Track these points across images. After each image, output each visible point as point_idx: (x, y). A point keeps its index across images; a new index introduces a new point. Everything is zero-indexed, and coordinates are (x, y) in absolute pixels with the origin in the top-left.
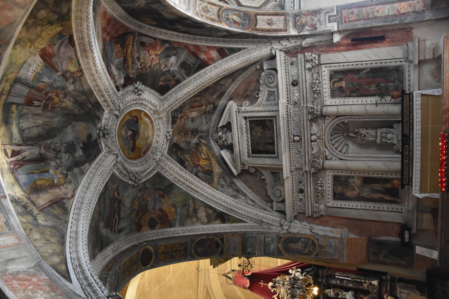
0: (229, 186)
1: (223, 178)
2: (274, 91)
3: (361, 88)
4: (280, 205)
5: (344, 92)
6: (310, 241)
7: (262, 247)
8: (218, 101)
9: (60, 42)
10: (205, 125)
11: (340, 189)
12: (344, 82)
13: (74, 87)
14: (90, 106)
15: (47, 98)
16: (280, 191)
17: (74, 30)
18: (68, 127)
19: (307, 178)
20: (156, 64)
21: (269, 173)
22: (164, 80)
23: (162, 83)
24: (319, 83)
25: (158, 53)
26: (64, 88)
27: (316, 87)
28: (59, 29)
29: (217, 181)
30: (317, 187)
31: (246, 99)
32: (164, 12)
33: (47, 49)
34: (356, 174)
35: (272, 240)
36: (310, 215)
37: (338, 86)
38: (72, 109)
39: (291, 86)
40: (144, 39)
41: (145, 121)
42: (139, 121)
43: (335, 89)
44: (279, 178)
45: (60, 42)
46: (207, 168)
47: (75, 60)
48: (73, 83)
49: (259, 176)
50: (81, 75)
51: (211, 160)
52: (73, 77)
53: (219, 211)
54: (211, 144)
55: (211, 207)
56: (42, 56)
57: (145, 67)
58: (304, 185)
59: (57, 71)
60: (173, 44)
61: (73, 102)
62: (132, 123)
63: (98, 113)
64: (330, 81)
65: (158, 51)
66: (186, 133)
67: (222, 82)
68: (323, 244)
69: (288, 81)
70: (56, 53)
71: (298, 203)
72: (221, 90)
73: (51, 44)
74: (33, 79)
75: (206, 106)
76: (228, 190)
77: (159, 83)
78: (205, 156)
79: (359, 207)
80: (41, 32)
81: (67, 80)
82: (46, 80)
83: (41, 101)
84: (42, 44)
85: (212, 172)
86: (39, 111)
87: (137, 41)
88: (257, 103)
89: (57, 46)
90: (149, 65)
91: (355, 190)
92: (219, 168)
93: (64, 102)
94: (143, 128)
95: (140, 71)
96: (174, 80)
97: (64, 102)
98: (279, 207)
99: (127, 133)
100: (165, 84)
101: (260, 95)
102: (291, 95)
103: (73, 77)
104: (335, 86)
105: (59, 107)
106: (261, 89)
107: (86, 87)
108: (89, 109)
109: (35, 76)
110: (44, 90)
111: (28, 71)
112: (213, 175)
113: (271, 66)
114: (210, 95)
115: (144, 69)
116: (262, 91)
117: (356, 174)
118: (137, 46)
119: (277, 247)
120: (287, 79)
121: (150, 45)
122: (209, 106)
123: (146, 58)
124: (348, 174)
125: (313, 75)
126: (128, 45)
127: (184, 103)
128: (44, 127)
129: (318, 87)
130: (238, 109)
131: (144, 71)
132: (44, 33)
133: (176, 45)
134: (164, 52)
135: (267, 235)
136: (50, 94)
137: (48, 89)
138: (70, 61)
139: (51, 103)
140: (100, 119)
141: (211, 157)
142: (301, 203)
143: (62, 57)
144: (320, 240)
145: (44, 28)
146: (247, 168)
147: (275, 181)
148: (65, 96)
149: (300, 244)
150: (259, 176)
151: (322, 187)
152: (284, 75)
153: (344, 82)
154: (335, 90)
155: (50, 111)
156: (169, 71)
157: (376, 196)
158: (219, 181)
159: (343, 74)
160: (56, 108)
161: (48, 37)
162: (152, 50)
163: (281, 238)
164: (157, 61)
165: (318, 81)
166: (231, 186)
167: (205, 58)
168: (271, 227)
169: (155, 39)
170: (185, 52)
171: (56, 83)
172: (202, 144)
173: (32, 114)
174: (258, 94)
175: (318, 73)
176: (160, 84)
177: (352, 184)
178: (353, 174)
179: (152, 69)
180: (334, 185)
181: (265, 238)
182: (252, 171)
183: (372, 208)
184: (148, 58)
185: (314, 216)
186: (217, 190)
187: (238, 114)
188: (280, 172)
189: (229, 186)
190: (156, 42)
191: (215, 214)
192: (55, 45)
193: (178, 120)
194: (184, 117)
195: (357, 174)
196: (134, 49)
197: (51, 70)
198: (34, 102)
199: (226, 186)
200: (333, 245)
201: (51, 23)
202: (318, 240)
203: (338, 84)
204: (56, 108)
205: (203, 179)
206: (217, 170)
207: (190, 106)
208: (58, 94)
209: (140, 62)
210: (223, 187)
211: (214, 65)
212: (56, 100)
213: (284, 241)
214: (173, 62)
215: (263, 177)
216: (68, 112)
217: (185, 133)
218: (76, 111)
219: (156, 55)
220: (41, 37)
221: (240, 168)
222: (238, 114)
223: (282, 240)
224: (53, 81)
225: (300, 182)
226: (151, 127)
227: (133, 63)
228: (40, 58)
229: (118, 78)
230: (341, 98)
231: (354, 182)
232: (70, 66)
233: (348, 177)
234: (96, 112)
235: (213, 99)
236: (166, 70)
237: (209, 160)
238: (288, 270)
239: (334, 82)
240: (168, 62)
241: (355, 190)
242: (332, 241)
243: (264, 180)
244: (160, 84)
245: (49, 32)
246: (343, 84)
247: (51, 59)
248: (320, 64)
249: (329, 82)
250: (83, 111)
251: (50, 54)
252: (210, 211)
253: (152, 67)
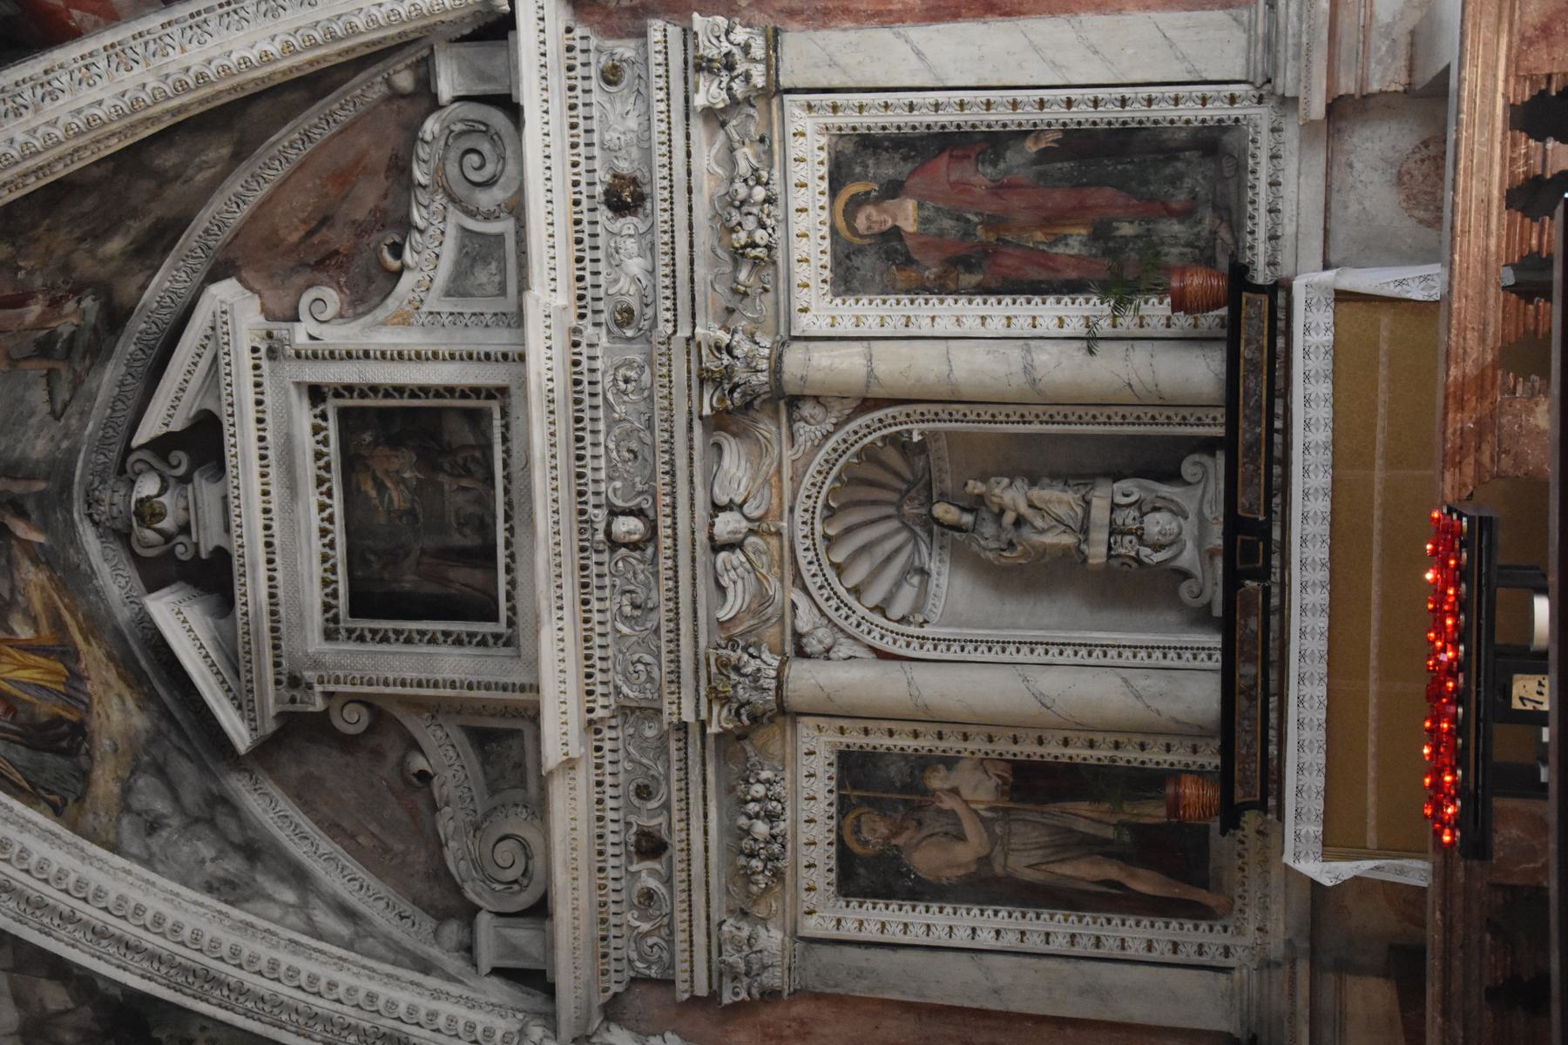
0: (192, 821)
1: (160, 771)
2: (500, 237)
3: (1006, 243)
4: (522, 935)
5: (908, 261)
8: (140, 279)
10: (41, 428)
11: (875, 831)
12: (910, 205)
16: (524, 846)
19: (685, 769)
21: (458, 736)
24: (769, 200)
27: (750, 223)
29: (116, 789)
30: (743, 821)
31: (323, 277)
34: (970, 746)
36: (702, 990)
37: (876, 229)
39: (604, 214)
43: (857, 240)
44: (520, 766)
46: (46, 709)
49: (393, 757)
51: (76, 655)
53: (118, 992)
54: (80, 550)
55: (58, 969)
58: (666, 806)
64: (834, 191)
67: (167, 159)
69: (583, 179)
71: (631, 918)
72: (158, 210)
75: (55, 303)
76: (186, 849)
78: (37, 631)
79: (986, 939)
85: (80, 731)
88: (392, 303)
91: (961, 838)
92: (131, 704)
98: (514, 950)
101: (408, 256)
102: (601, 267)
104: (861, 223)
106: (417, 216)
112: (88, 753)
113: (483, 77)
114: (77, 233)
116: (421, 232)
117: (970, 746)
120: (582, 168)
122: (70, 306)
124: (926, 743)
125: (732, 150)
129: (763, 226)
130: (270, 335)
141: (78, 638)
142: (647, 918)
146: (319, 705)
147: (493, 789)
150: (393, 757)
151: (771, 817)
152: (560, 141)
153: (910, 205)
154: (860, 251)
157: (1084, 871)
158: (127, 790)
159: (905, 159)
165: (759, 193)
166: (212, 823)
172: (17, 551)
174: (397, 250)
175: (762, 140)
177: (948, 803)
178: (952, 744)
180: (844, 806)
182: (353, 721)
183: (1059, 944)
185: (727, 998)
186: (115, 848)
187: (265, 365)
188: (528, 730)
189: (197, 820)
191: (87, 1012)
195: (977, 745)
199: (175, 822)
203: (875, 216)
205: (17, 777)
206: (116, 716)
210: (153, 826)
211: (108, 37)
215: (419, 763)
221: (271, 701)
222: (265, 365)
225: (644, 792)
230: (892, 299)
231: (955, 791)
233: (924, 763)
235: (103, 262)
237: (64, 652)
239: (856, 203)
241: (961, 838)
243: (424, 777)
246: (906, 215)
248: (775, 91)
249: (825, 200)
252: (55, 996)
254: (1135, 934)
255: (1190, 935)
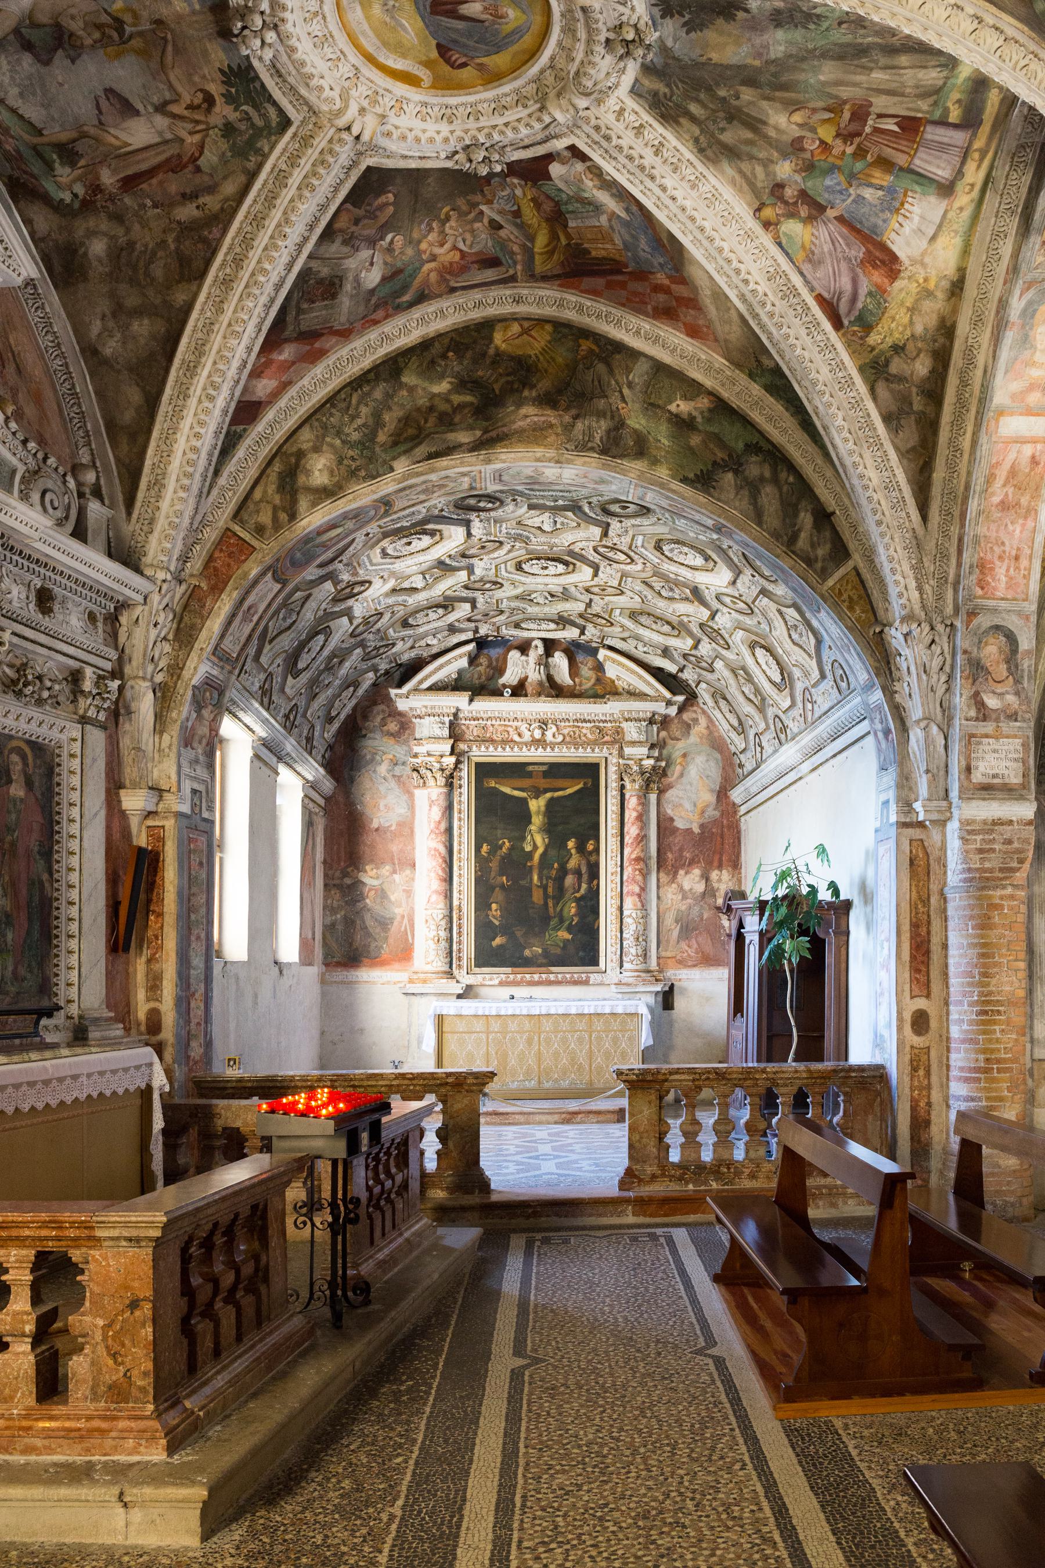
9: (860, 305)
13: (775, 174)
14: (694, 108)
15: (857, 140)
17: (840, 346)
18: (780, 55)
20: (426, 237)
22: (378, 213)
23: (382, 199)
25: (427, 267)
26: (809, 168)
28: (874, 339)
32: (553, 420)
33: (886, 281)
38: (764, 104)
40: (490, 274)
41: (404, 56)
42: (434, 54)
45: (860, 305)
47: (800, 256)
48: (779, 186)
50: (758, 210)
52: (786, 203)
56: (894, 258)
57: (462, 215)
59: (840, 219)
60: (391, 311)
61: (765, 123)
62: (471, 43)
63: (650, 84)
65: (431, 271)
66: (115, 35)
67: (142, 328)
70: (858, 270)
73: (879, 293)
74: (905, 195)
77: (395, 196)
80: (911, 323)
81: (803, 194)
82: (868, 193)
83: (876, 130)
84: (901, 290)
86: (880, 103)
87: (515, 263)
89: (863, 291)
90: (452, 223)
93: (800, 125)
94: (405, 30)
95: (478, 198)
96: (341, 231)
97: (800, 125)
99: (485, 8)
100: (370, 205)
103: (786, 203)
105: (814, 110)
107: (730, 171)
108: (697, 100)
109: (902, 204)
110: (871, 165)
111: (922, 217)
115: (464, 208)
118: (512, 253)
121: (463, 269)
123: (468, 236)
126: (551, 253)
127: (253, 176)
128: (872, 65)
131: (461, 202)
132: (906, 320)
133: (380, 314)
134: (410, 276)
136: (850, 150)
137: (859, 166)
138: (813, 253)
139: (842, 125)
140: (647, 69)
143: (838, 262)
145: (908, 333)
148: (796, 146)
155: (845, 102)
156: (372, 243)
160: (824, 109)
161: (893, 312)
162: (451, 263)
164: (424, 246)
167: (280, 354)
169: (453, 290)
170: (343, 319)
171: (838, 184)
173: (903, 95)
176: (390, 195)
179: (437, 217)
184: (460, 239)
190: (448, 286)
192: (870, 294)
193: (215, 89)
194: (190, 107)
196: (523, 246)
197: (861, 223)
198: (896, 128)
201: (898, 349)
204: (824, 109)
207: (198, 170)
208: (822, 152)
209: (486, 221)
212: (826, 133)
214: (368, 271)
216: (777, 94)
217: (121, 31)
218: (747, 94)
219: (433, 258)
220: (908, 309)
224: (847, 190)
226: (363, 41)
227: (517, 214)
228: (899, 253)
229: (581, 181)
232: (807, 238)
234: (663, 89)
235: (91, 234)
236: (382, 238)
240: (386, 263)
244: (390, 195)
245: (893, 325)
247: (868, 252)
250: (722, 93)
251: (875, 266)
253: (434, 225)
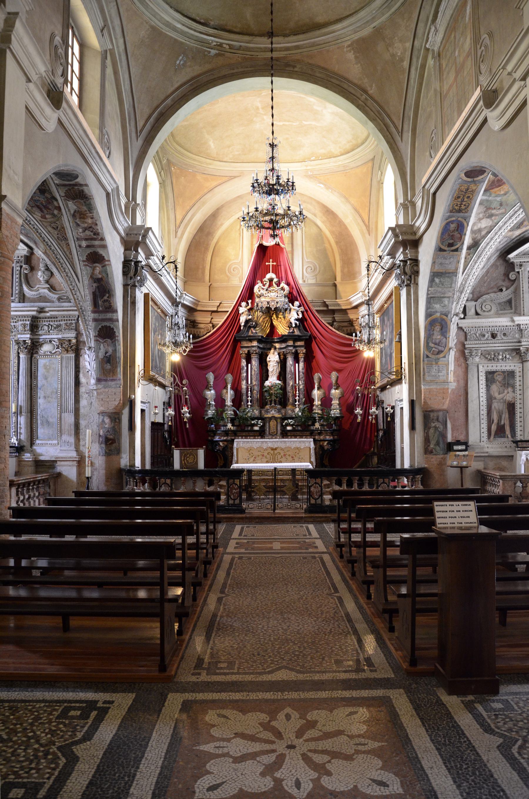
4: (473, 311)
6: (443, 349)
7: (438, 295)
11: (499, 378)
16: (490, 311)
19: (509, 343)
21: (510, 297)
30: (501, 353)
34: (518, 395)
35: (445, 306)
36: (466, 346)
44: (505, 309)
49: (504, 284)
58: (502, 339)
68: (440, 363)
71: (479, 332)
79: (481, 399)
91: (499, 394)
98: (470, 310)
117: (518, 395)
119: (436, 312)
124: (518, 387)
135: (451, 300)
142: (479, 335)
144: (444, 359)
146: (517, 270)
147: (499, 304)
149: (439, 337)
150: (504, 284)
151: (502, 359)
157: (495, 417)
163: (447, 316)
168: (455, 303)
177: (506, 391)
178: (518, 392)
180: (504, 372)
181: (449, 297)
182: (512, 276)
183: (482, 412)
185: (466, 351)
188: (513, 311)
195: (519, 397)
200: (440, 374)
202: (445, 357)
213: (443, 320)
215: (504, 289)
221: (517, 261)
223: (445, 317)
225: (505, 335)
231: (508, 393)
233: (513, 387)
238: (297, 300)
241: (499, 394)
242: (444, 372)
243: (501, 290)
254: (485, 426)
255: (485, 435)
